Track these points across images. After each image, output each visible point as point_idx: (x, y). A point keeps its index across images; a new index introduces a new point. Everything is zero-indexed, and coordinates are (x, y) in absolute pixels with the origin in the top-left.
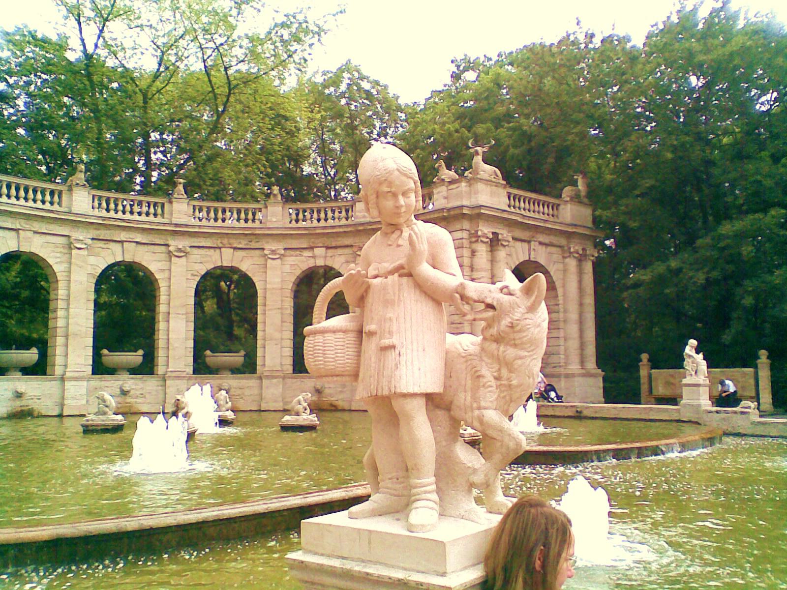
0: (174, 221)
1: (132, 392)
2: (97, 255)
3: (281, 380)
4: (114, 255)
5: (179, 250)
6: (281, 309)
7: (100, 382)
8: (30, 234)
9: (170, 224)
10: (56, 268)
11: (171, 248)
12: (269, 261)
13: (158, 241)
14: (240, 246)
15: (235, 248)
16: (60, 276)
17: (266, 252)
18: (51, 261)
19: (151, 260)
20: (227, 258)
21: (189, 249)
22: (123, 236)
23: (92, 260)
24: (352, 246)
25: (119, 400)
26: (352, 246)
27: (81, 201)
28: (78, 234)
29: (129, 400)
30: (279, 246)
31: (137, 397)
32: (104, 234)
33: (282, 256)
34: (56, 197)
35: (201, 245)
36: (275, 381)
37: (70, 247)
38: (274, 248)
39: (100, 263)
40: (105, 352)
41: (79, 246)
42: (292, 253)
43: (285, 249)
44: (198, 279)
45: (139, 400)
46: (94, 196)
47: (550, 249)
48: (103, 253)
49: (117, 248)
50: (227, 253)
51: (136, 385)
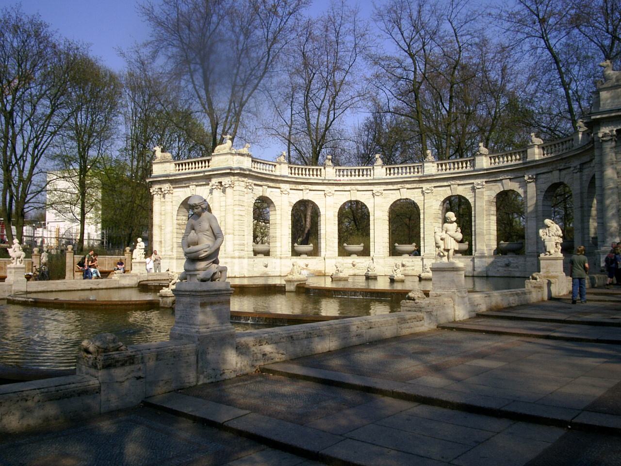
1: (512, 265)
4: (499, 188)
7: (296, 259)
9: (423, 176)
11: (374, 192)
12: (575, 175)
14: (561, 168)
15: (560, 170)
16: (472, 205)
25: (506, 269)
28: (476, 181)
30: (576, 163)
31: (514, 268)
33: (581, 170)
35: (542, 172)
37: (474, 189)
38: (575, 165)
41: (478, 187)
44: (543, 193)
46: (490, 157)
48: (494, 188)
49: (500, 184)
51: (513, 260)
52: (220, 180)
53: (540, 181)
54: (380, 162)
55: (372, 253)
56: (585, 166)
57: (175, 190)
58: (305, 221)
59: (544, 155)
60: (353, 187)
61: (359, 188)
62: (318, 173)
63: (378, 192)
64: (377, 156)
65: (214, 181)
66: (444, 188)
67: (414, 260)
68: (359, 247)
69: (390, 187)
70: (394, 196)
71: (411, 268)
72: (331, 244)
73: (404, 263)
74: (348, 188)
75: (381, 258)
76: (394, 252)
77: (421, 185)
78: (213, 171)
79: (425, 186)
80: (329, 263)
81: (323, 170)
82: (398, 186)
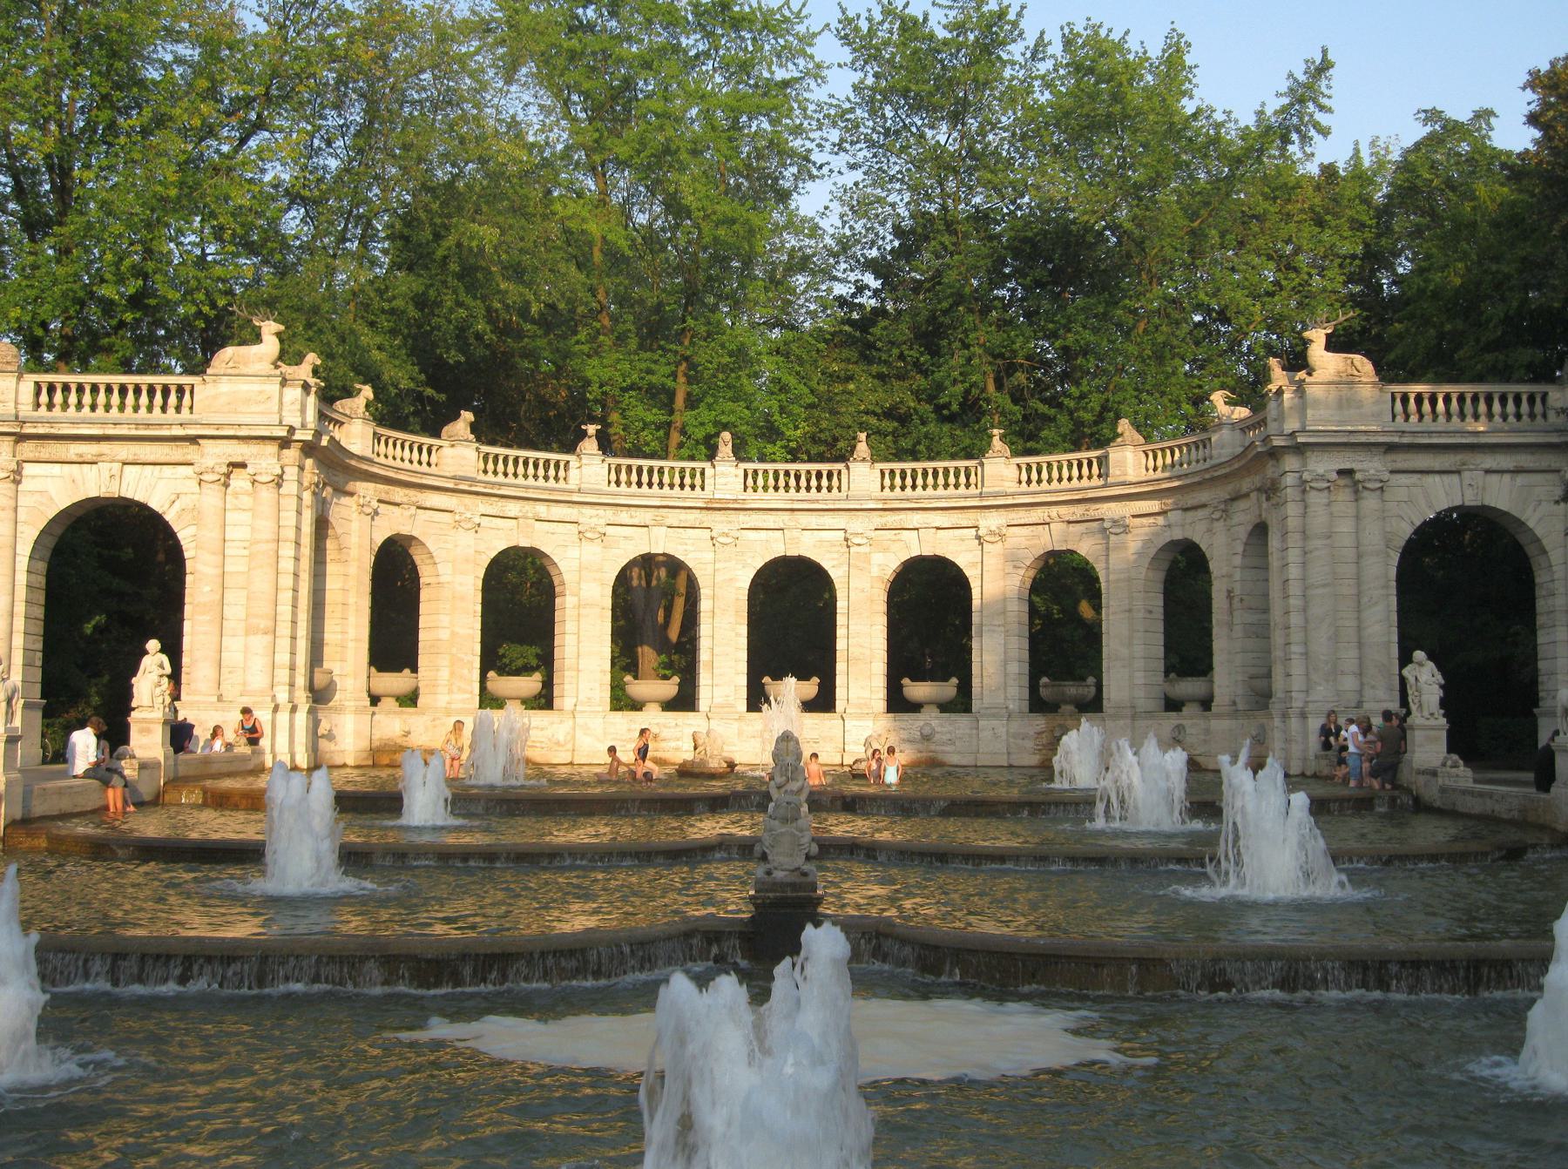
2: (886, 550)
3: (1128, 721)
5: (992, 533)
6: (1130, 611)
8: (796, 533)
12: (1112, 537)
17: (1106, 525)
18: (826, 565)
21: (1004, 531)
22: (916, 519)
23: (878, 558)
24: (1204, 506)
26: (1204, 506)
28: (857, 524)
29: (933, 747)
31: (944, 744)
36: (1122, 722)
40: (906, 681)
41: (857, 540)
45: (948, 748)
47: (1521, 479)
52: (237, 451)
54: (589, 446)
55: (840, 704)
57: (29, 469)
58: (668, 617)
60: (528, 506)
61: (542, 510)
62: (696, 481)
63: (593, 529)
64: (592, 429)
65: (215, 455)
67: (680, 721)
69: (624, 516)
71: (673, 744)
72: (466, 672)
74: (513, 508)
78: (219, 426)
80: (584, 726)
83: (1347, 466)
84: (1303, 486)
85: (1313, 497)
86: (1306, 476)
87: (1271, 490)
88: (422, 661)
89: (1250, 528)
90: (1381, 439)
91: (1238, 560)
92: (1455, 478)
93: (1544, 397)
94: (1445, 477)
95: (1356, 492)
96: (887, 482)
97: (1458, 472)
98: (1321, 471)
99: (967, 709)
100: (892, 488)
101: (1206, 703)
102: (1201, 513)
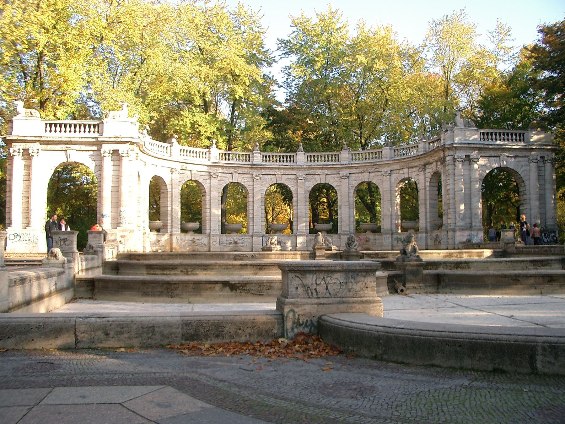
0: (342, 163)
2: (309, 181)
10: (292, 189)
13: (335, 173)
19: (333, 181)
20: (365, 177)
22: (319, 172)
27: (301, 157)
28: (300, 173)
30: (387, 169)
32: (311, 172)
33: (390, 175)
34: (292, 158)
39: (311, 185)
42: (395, 172)
43: (391, 171)
47: (517, 159)
50: (366, 174)
53: (351, 179)
56: (393, 172)
59: (352, 160)
63: (215, 174)
66: (269, 176)
68: (196, 225)
70: (228, 180)
73: (236, 240)
75: (217, 235)
76: (224, 230)
77: (252, 171)
79: (255, 173)
81: (169, 148)
82: (232, 170)
83: (468, 154)
84: (454, 160)
85: (457, 163)
86: (456, 157)
87: (443, 161)
88: (161, 218)
89: (432, 174)
90: (478, 146)
91: (428, 184)
92: (498, 158)
93: (523, 134)
94: (495, 158)
95: (470, 162)
96: (309, 159)
97: (499, 157)
98: (460, 155)
99: (337, 233)
100: (311, 161)
101: (417, 230)
102: (414, 169)
